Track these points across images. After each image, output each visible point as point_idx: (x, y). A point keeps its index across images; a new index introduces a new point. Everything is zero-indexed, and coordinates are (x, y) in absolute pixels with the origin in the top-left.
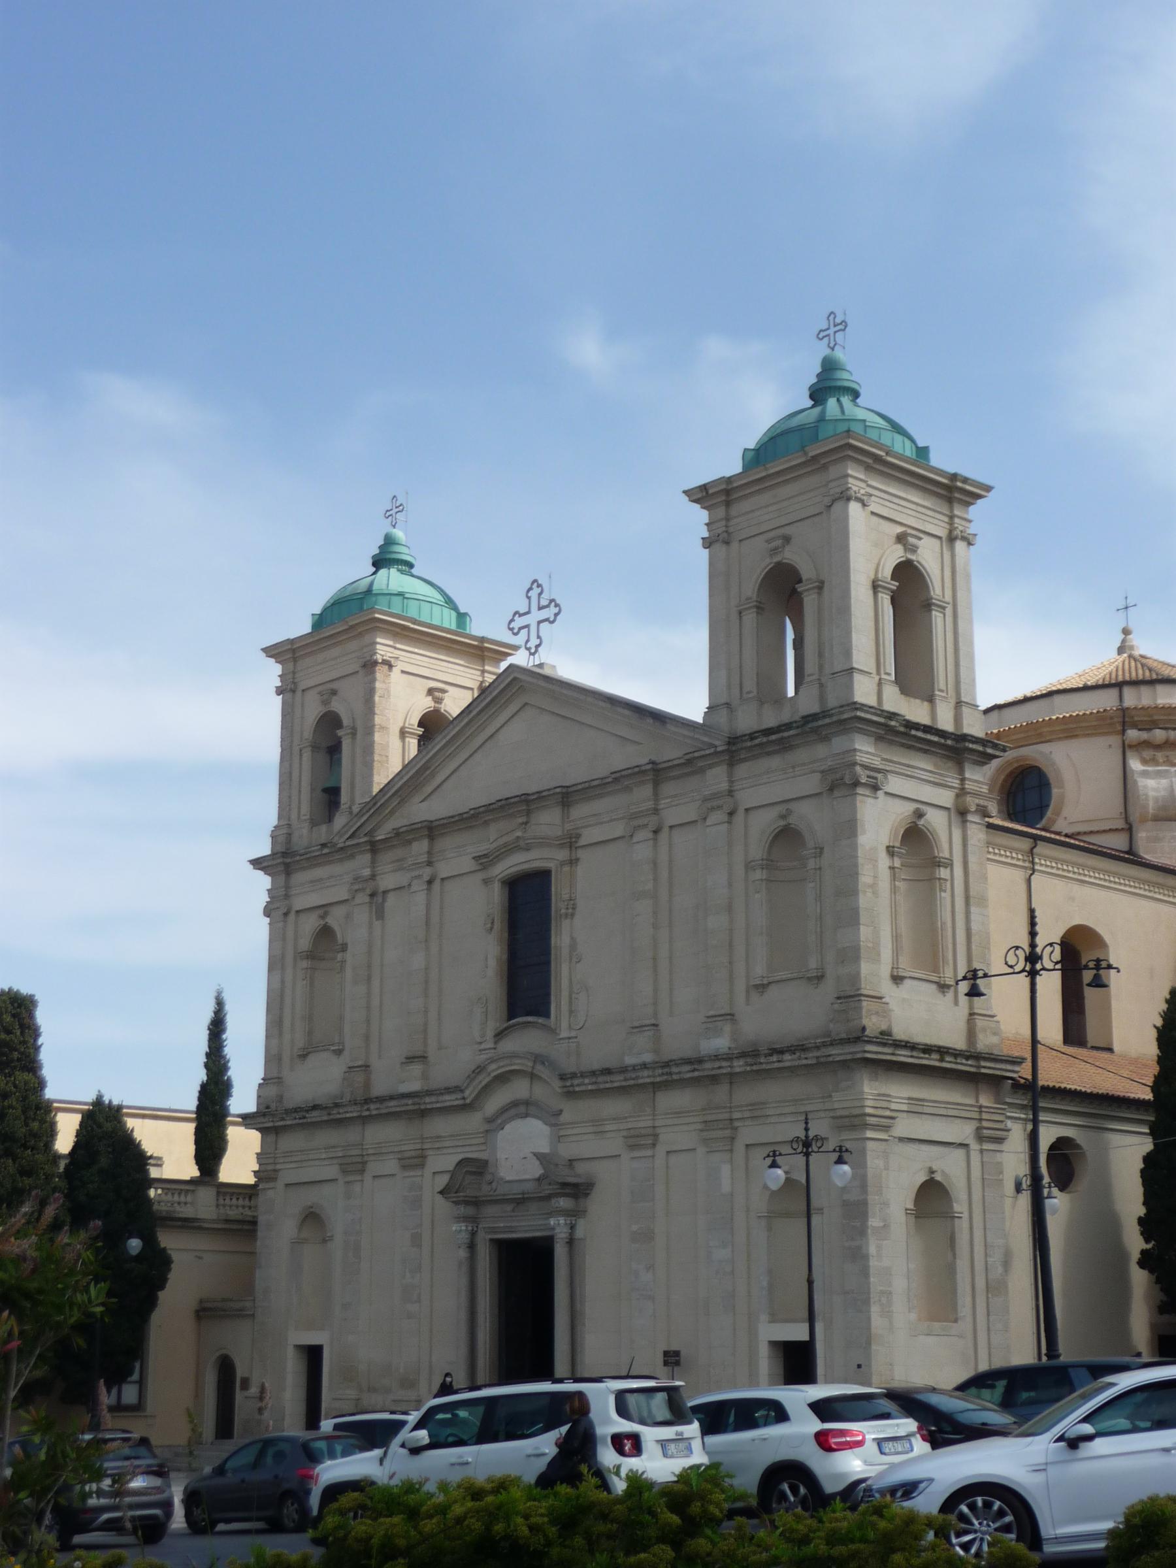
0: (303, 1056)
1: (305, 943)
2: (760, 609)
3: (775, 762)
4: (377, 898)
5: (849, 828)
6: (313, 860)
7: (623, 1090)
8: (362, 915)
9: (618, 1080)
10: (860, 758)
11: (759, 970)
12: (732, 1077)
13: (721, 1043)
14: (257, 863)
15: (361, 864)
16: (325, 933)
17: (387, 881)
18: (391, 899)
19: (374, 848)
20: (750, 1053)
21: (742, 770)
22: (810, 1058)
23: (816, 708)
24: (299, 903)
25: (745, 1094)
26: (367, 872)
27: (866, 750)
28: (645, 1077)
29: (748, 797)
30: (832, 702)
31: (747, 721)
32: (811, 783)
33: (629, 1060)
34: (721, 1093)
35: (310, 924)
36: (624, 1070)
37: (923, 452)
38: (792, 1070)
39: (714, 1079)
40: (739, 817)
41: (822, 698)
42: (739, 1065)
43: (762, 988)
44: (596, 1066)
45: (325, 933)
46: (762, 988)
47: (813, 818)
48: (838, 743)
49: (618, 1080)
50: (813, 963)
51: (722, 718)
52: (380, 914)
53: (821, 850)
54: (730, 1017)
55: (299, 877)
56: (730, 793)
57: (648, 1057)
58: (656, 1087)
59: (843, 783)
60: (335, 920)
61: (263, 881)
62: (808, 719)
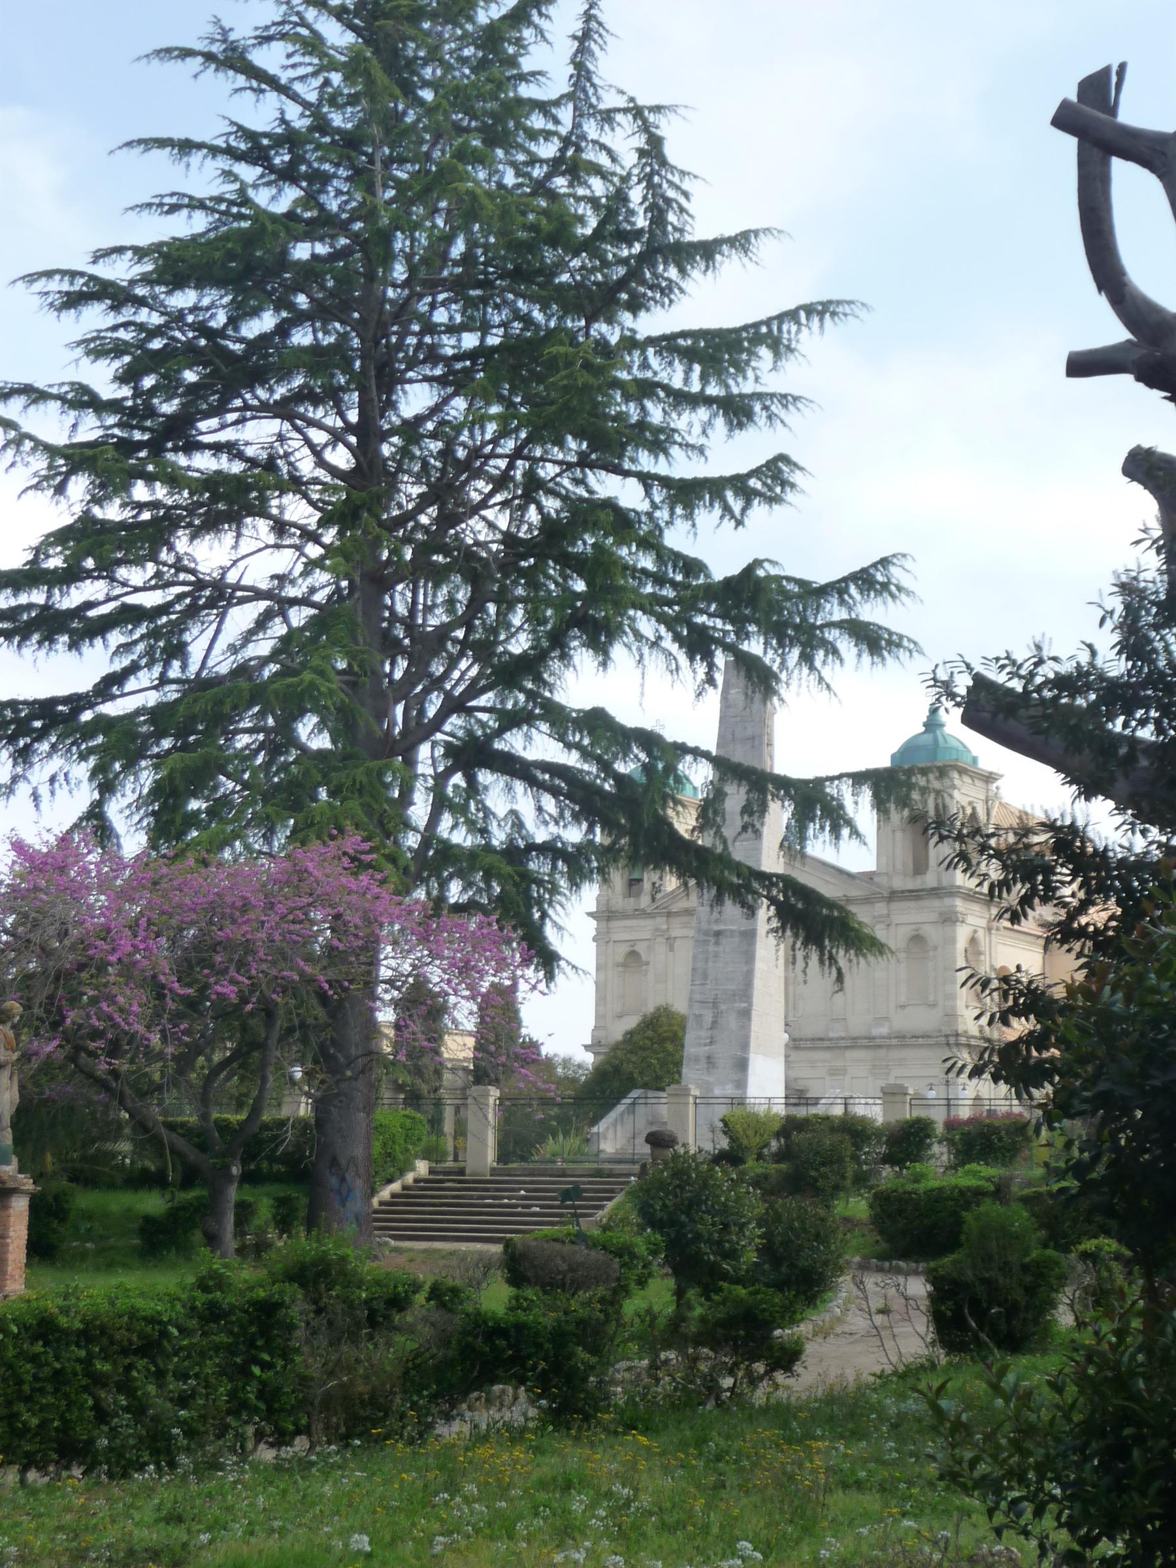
0: (620, 1017)
1: (620, 958)
2: (904, 830)
3: (912, 904)
4: (670, 941)
5: (953, 940)
6: (625, 916)
7: (828, 1048)
8: (661, 948)
9: (826, 1044)
10: (959, 909)
11: (903, 999)
12: (889, 1047)
13: (883, 1030)
14: (590, 914)
15: (661, 923)
16: (633, 954)
17: (676, 932)
18: (678, 943)
19: (669, 915)
20: (901, 1037)
21: (895, 906)
22: (932, 1041)
23: (935, 885)
24: (615, 937)
25: (895, 1054)
26: (664, 927)
27: (960, 904)
28: (842, 1043)
29: (897, 918)
30: (945, 883)
31: (899, 883)
32: (933, 917)
33: (831, 1035)
34: (882, 1053)
35: (623, 949)
36: (830, 1039)
37: (975, 760)
38: (921, 1046)
39: (879, 1047)
40: (892, 928)
41: (939, 880)
42: (894, 1042)
43: (903, 1007)
44: (810, 1036)
45: (633, 954)
46: (903, 1007)
47: (932, 933)
48: (947, 901)
49: (826, 1044)
50: (931, 998)
51: (883, 880)
52: (671, 949)
53: (935, 948)
54: (887, 1019)
55: (615, 924)
56: (888, 916)
57: (843, 1034)
58: (847, 1048)
59: (950, 919)
60: (641, 948)
61: (593, 923)
62: (933, 889)
